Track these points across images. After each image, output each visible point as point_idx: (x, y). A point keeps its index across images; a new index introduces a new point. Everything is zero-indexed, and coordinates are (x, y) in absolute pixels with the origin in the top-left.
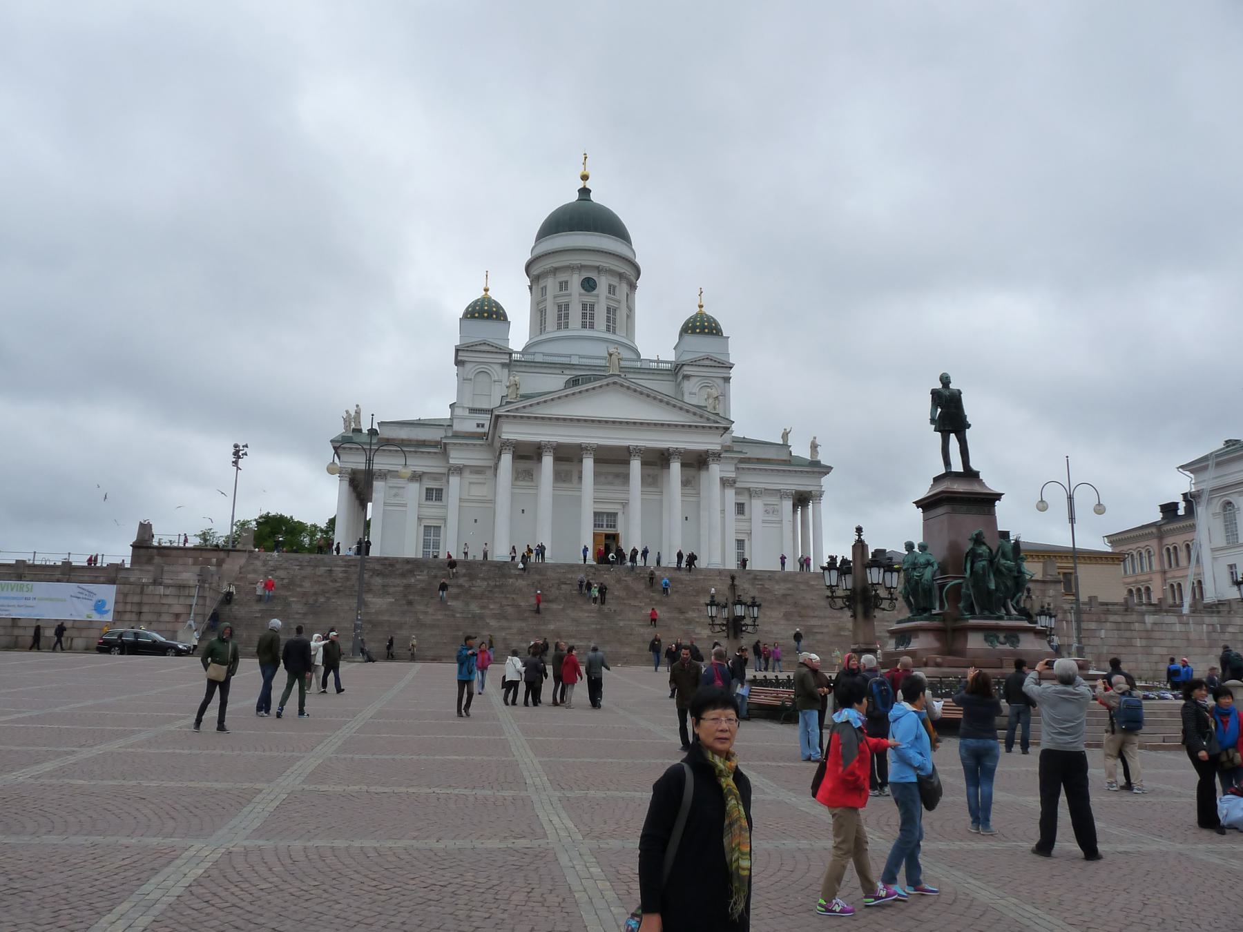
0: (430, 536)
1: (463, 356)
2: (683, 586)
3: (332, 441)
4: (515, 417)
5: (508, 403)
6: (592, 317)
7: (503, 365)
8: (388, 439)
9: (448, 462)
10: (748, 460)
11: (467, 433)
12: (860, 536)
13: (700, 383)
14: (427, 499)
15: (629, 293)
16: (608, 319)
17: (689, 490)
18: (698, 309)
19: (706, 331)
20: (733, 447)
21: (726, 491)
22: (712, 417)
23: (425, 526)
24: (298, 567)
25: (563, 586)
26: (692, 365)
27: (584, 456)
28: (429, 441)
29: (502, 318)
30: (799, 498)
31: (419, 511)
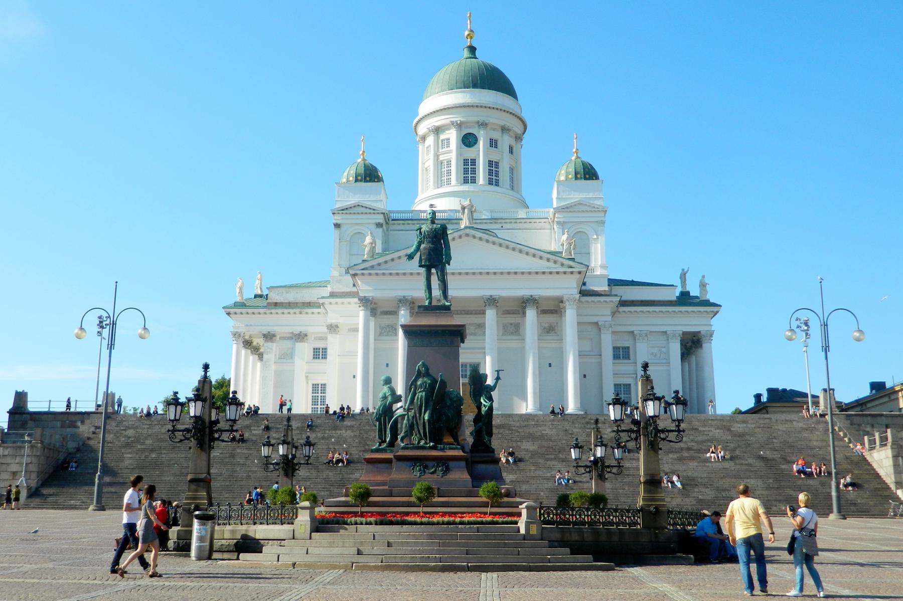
0: (318, 393)
2: (510, 432)
3: (223, 308)
5: (364, 261)
6: (474, 171)
7: (379, 225)
8: (276, 303)
10: (632, 303)
11: (343, 292)
12: (206, 373)
14: (314, 358)
16: (490, 173)
21: (603, 336)
22: (566, 262)
24: (148, 426)
29: (376, 180)
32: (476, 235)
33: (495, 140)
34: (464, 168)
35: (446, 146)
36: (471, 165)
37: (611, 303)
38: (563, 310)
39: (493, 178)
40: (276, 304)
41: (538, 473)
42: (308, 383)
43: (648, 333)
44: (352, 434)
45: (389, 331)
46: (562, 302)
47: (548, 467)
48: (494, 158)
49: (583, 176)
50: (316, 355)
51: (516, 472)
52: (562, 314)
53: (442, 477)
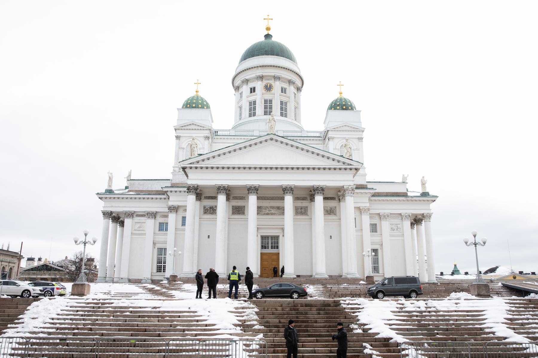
3: (98, 194)
4: (196, 168)
6: (271, 108)
7: (207, 138)
13: (341, 142)
14: (159, 230)
15: (296, 93)
16: (282, 109)
17: (332, 217)
18: (339, 95)
20: (367, 185)
21: (363, 216)
23: (158, 248)
26: (334, 131)
29: (205, 107)
30: (415, 219)
31: (154, 238)
33: (284, 89)
34: (265, 105)
35: (253, 92)
36: (269, 103)
39: (284, 112)
42: (155, 248)
43: (389, 214)
48: (284, 99)
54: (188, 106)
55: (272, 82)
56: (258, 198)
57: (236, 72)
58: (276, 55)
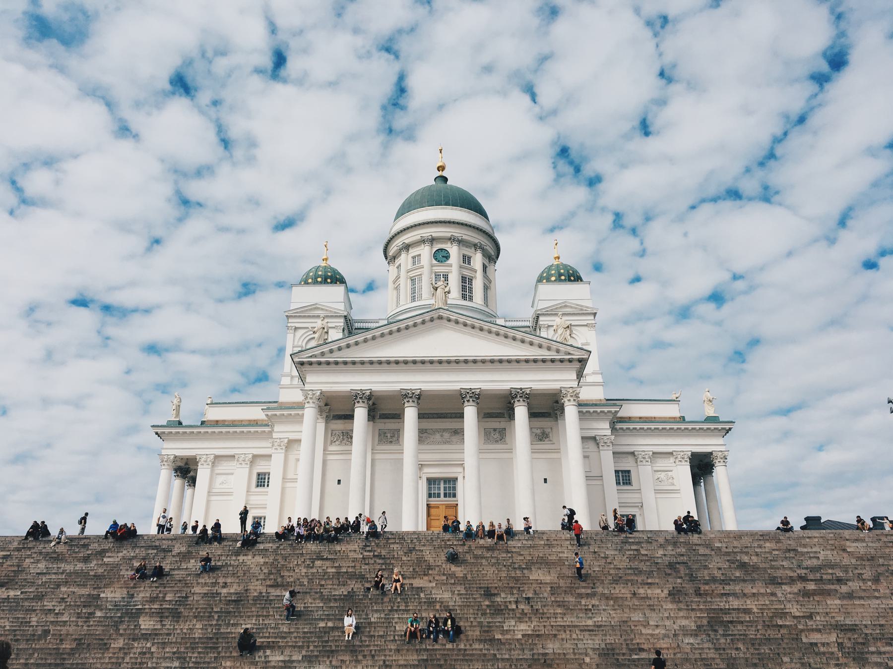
1: (294, 323)
2: (509, 555)
3: (153, 426)
4: (320, 363)
8: (217, 421)
9: (272, 438)
11: (294, 403)
14: (257, 486)
16: (464, 288)
17: (545, 445)
19: (563, 278)
22: (562, 348)
25: (318, 563)
27: (406, 405)
28: (263, 420)
29: (338, 283)
30: (699, 464)
32: (451, 317)
37: (609, 414)
38: (559, 413)
40: (217, 423)
41: (569, 620)
44: (262, 561)
45: (343, 439)
46: (557, 402)
47: (586, 610)
49: (567, 278)
50: (261, 482)
51: (530, 618)
52: (557, 417)
53: (237, 553)
54: (310, 281)
55: (447, 246)
56: (421, 416)
57: (392, 232)
58: (453, 206)
